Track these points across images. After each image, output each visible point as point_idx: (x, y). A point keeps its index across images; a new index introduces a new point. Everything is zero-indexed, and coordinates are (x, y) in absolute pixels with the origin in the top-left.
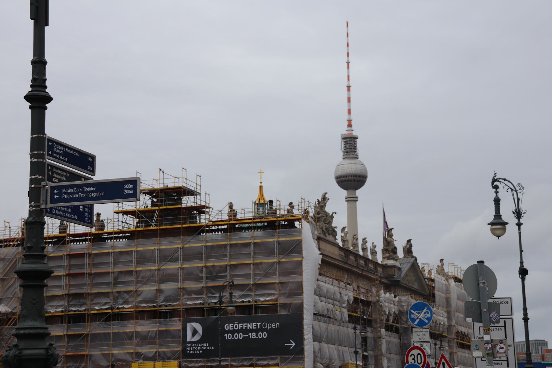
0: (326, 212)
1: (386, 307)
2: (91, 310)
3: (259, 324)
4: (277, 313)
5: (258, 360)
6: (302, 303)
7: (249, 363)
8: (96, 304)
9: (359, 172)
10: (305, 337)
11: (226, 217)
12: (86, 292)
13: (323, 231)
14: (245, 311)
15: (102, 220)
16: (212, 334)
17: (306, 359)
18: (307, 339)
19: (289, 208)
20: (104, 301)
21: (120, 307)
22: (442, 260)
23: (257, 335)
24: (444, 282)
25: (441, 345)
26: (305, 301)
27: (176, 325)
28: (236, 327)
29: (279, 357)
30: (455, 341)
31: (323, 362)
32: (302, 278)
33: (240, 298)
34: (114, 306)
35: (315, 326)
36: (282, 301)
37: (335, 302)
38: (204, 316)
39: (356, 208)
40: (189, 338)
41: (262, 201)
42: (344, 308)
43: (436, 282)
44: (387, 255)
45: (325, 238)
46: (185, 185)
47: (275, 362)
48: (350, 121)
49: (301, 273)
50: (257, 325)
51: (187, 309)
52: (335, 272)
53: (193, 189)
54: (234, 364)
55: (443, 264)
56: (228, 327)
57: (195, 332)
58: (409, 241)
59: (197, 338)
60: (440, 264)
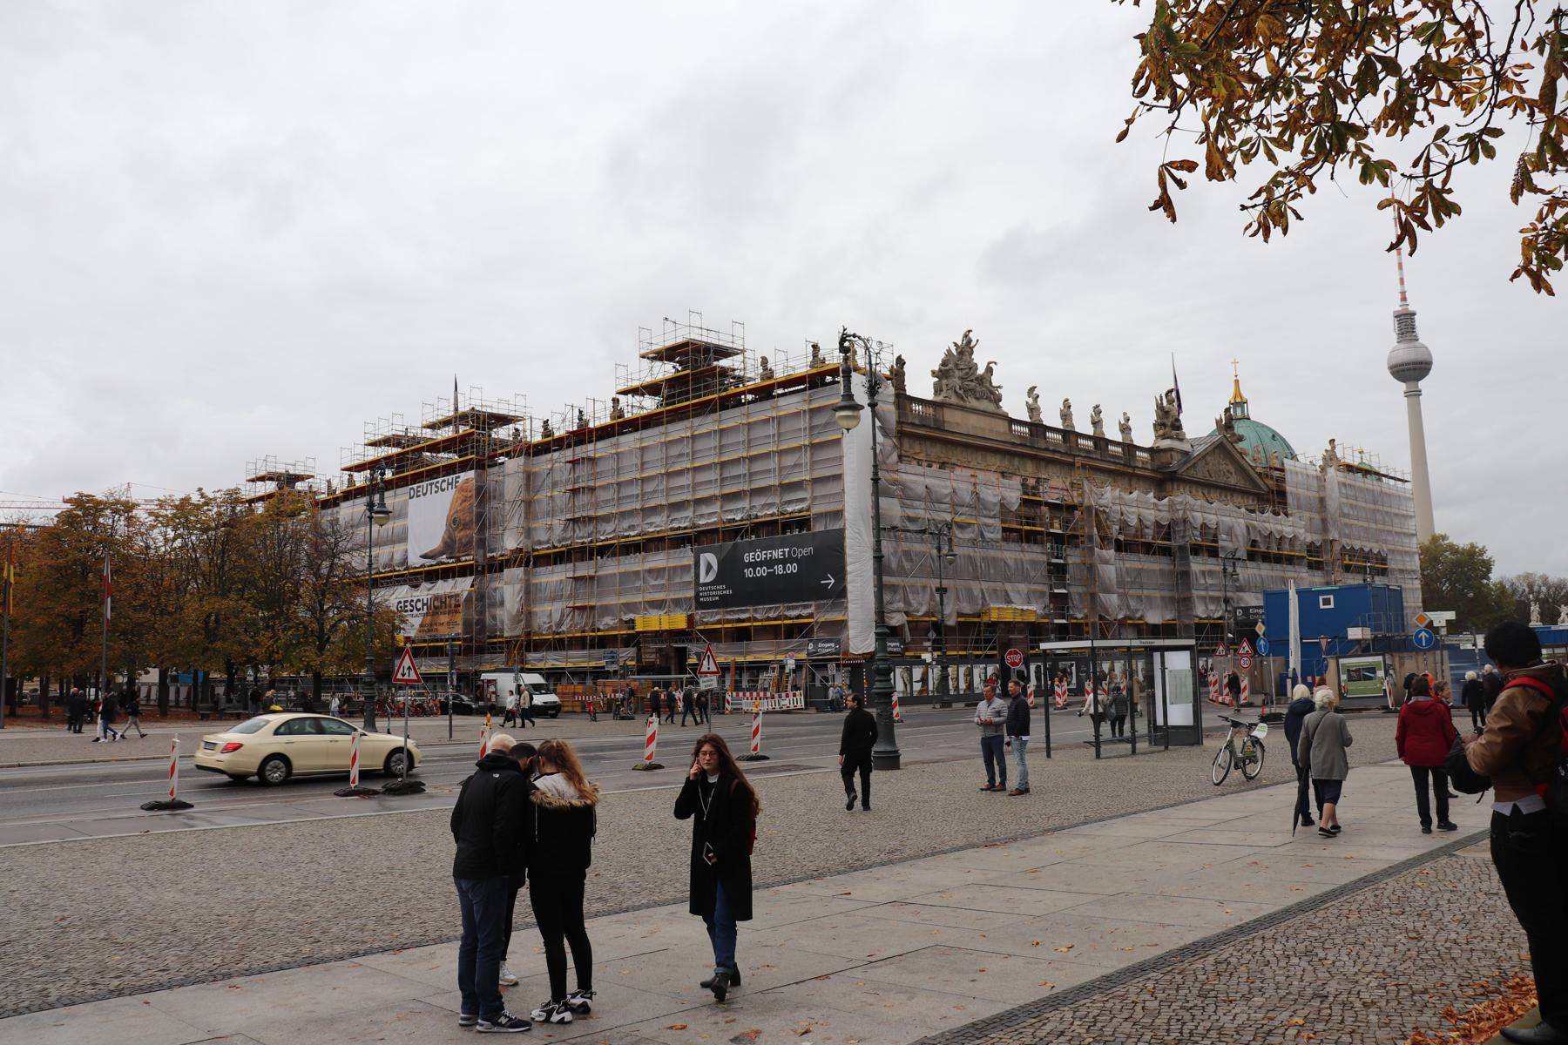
5: (789, 609)
9: (1420, 358)
10: (849, 568)
16: (729, 570)
22: (1332, 441)
27: (685, 557)
33: (765, 509)
39: (1419, 404)
42: (994, 517)
48: (1403, 293)
52: (996, 462)
54: (758, 616)
56: (748, 557)
57: (709, 567)
59: (711, 577)
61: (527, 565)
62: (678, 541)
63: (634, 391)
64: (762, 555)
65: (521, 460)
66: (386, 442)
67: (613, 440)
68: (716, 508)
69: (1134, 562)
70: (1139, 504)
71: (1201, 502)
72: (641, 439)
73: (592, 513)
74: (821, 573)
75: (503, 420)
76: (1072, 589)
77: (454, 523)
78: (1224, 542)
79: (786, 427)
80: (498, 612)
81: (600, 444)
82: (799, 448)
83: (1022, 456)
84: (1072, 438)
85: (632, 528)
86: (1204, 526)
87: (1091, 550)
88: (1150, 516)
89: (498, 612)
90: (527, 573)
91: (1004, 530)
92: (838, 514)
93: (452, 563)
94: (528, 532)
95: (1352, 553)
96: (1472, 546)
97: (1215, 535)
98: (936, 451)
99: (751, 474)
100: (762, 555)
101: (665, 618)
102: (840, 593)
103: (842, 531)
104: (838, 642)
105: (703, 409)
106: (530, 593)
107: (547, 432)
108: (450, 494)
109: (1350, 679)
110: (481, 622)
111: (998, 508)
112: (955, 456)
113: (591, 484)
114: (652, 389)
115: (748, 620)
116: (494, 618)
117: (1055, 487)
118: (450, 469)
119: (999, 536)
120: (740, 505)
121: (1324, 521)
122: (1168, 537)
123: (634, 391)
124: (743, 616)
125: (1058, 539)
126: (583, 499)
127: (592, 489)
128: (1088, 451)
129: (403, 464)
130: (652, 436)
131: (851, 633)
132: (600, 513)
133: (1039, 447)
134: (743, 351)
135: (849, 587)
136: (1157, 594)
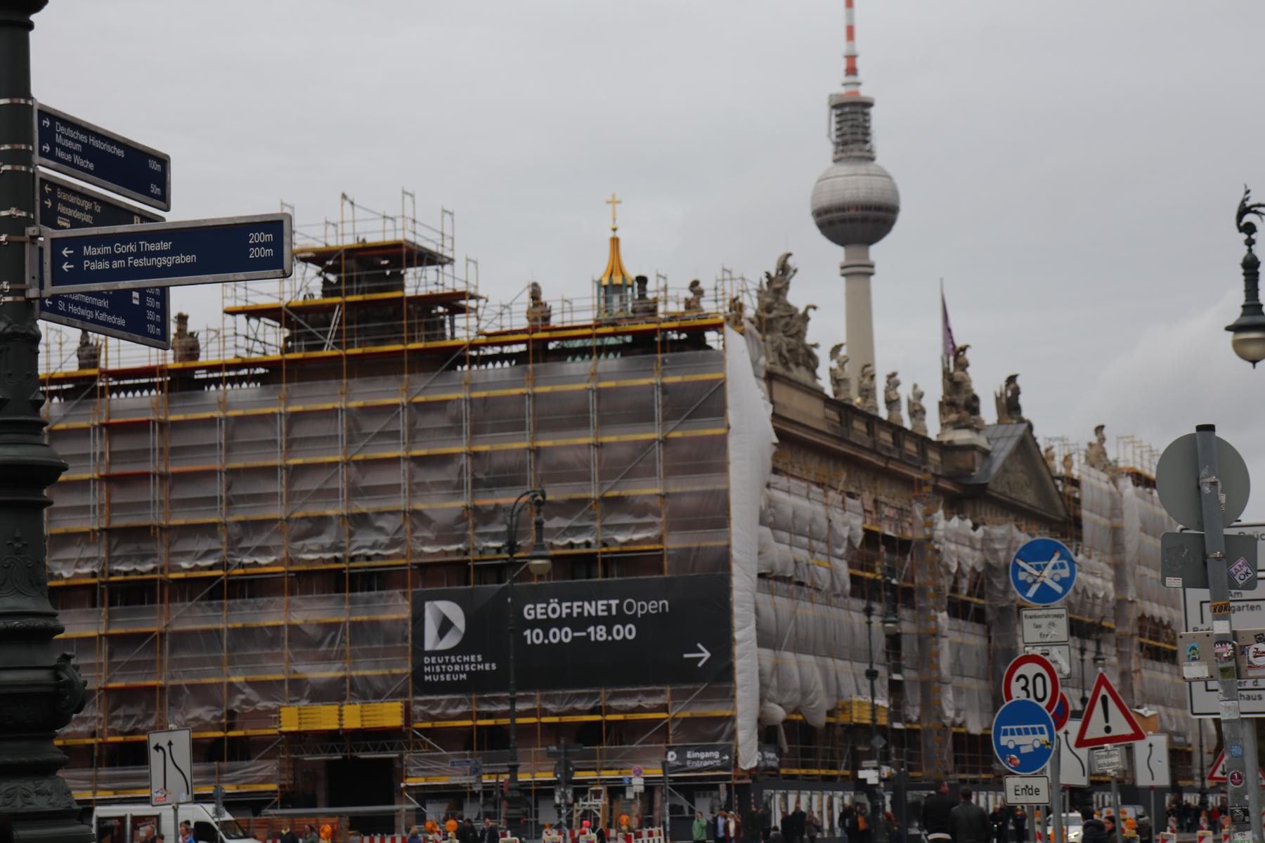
0: (789, 306)
1: (952, 552)
2: (171, 571)
3: (614, 603)
4: (661, 572)
5: (614, 696)
6: (728, 546)
7: (591, 705)
8: (183, 554)
9: (877, 197)
10: (737, 635)
11: (522, 323)
12: (156, 523)
13: (781, 355)
14: (577, 569)
15: (192, 334)
16: (490, 630)
18: (742, 641)
19: (690, 295)
20: (203, 546)
21: (246, 560)
22: (1099, 429)
23: (609, 632)
24: (1105, 487)
25: (1098, 652)
28: (554, 611)
29: (668, 689)
30: (1136, 640)
31: (785, 700)
32: (727, 482)
34: (229, 560)
35: (762, 608)
36: (673, 543)
37: (814, 543)
38: (467, 583)
39: (868, 293)
40: (431, 641)
41: (618, 280)
42: (840, 558)
43: (1083, 486)
44: (953, 417)
45: (787, 373)
46: (410, 238)
47: (659, 701)
48: (851, 58)
49: (723, 468)
50: (609, 606)
51: (423, 567)
52: (814, 466)
53: (432, 247)
54: (550, 707)
55: (1102, 440)
57: (445, 626)
58: (1011, 380)
59: (450, 641)
60: (1094, 440)
85: (262, 550)
91: (854, 578)
102: (720, 675)
104: (724, 750)
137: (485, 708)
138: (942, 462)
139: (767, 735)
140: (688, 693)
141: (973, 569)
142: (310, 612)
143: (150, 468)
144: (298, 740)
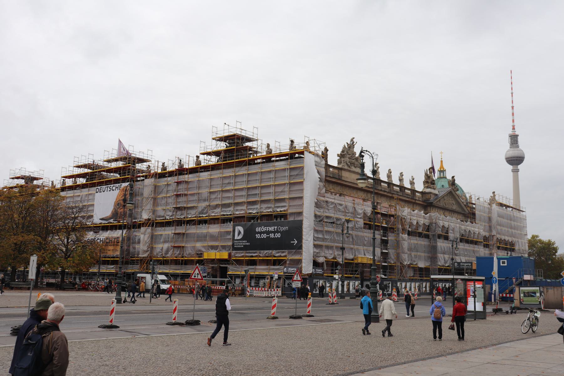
0: (353, 151)
9: (519, 155)
10: (304, 237)
11: (265, 154)
12: (182, 206)
16: (249, 234)
17: (303, 253)
22: (494, 193)
26: (304, 211)
27: (229, 227)
30: (495, 245)
33: (266, 209)
36: (290, 211)
39: (518, 175)
41: (442, 169)
42: (360, 218)
44: (426, 185)
45: (349, 169)
52: (361, 194)
54: (261, 255)
55: (495, 196)
56: (258, 229)
57: (239, 233)
58: (453, 177)
59: (240, 237)
61: (153, 226)
62: (225, 220)
63: (208, 154)
64: (264, 229)
65: (153, 180)
66: (85, 166)
67: (197, 174)
68: (244, 207)
69: (415, 241)
70: (418, 216)
71: (443, 216)
72: (211, 175)
73: (185, 205)
74: (291, 238)
75: (142, 161)
76: (390, 251)
77: (117, 204)
78: (451, 235)
79: (278, 175)
80: (137, 246)
81: (190, 176)
82: (285, 184)
83: (371, 192)
84: (391, 186)
86: (443, 226)
87: (398, 234)
88: (422, 221)
89: (137, 246)
90: (152, 230)
91: (365, 224)
92: (300, 214)
93: (116, 223)
94: (154, 212)
95: (500, 241)
96: (549, 241)
97: (447, 231)
98: (338, 189)
99: (261, 194)
100: (264, 229)
101: (218, 254)
102: (299, 247)
103: (301, 222)
105: (240, 164)
106: (153, 238)
107: (164, 168)
108: (117, 192)
109: (525, 296)
110: (128, 250)
111: (362, 214)
112: (346, 191)
113: (186, 192)
114: (217, 153)
115: (256, 256)
116: (134, 248)
117: (384, 207)
118: (116, 181)
119: (363, 226)
120: (256, 207)
121: (490, 227)
122: (428, 230)
123: (208, 154)
124: (254, 255)
125: (385, 229)
126: (181, 199)
127: (186, 195)
128: (397, 192)
129: (94, 177)
130: (216, 174)
131: (303, 265)
132: (189, 206)
133: (377, 189)
134: (257, 140)
135: (304, 245)
136: (423, 254)
137: (247, 255)
138: (422, 197)
139: (316, 264)
140: (292, 252)
141: (424, 224)
142: (214, 229)
143: (182, 193)
144: (212, 261)
